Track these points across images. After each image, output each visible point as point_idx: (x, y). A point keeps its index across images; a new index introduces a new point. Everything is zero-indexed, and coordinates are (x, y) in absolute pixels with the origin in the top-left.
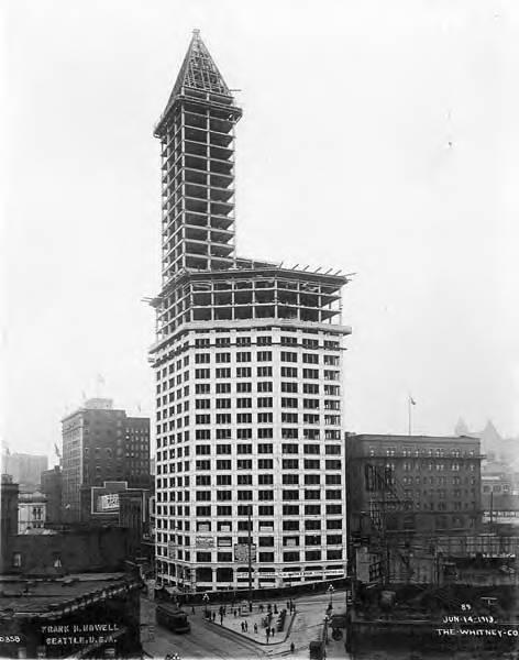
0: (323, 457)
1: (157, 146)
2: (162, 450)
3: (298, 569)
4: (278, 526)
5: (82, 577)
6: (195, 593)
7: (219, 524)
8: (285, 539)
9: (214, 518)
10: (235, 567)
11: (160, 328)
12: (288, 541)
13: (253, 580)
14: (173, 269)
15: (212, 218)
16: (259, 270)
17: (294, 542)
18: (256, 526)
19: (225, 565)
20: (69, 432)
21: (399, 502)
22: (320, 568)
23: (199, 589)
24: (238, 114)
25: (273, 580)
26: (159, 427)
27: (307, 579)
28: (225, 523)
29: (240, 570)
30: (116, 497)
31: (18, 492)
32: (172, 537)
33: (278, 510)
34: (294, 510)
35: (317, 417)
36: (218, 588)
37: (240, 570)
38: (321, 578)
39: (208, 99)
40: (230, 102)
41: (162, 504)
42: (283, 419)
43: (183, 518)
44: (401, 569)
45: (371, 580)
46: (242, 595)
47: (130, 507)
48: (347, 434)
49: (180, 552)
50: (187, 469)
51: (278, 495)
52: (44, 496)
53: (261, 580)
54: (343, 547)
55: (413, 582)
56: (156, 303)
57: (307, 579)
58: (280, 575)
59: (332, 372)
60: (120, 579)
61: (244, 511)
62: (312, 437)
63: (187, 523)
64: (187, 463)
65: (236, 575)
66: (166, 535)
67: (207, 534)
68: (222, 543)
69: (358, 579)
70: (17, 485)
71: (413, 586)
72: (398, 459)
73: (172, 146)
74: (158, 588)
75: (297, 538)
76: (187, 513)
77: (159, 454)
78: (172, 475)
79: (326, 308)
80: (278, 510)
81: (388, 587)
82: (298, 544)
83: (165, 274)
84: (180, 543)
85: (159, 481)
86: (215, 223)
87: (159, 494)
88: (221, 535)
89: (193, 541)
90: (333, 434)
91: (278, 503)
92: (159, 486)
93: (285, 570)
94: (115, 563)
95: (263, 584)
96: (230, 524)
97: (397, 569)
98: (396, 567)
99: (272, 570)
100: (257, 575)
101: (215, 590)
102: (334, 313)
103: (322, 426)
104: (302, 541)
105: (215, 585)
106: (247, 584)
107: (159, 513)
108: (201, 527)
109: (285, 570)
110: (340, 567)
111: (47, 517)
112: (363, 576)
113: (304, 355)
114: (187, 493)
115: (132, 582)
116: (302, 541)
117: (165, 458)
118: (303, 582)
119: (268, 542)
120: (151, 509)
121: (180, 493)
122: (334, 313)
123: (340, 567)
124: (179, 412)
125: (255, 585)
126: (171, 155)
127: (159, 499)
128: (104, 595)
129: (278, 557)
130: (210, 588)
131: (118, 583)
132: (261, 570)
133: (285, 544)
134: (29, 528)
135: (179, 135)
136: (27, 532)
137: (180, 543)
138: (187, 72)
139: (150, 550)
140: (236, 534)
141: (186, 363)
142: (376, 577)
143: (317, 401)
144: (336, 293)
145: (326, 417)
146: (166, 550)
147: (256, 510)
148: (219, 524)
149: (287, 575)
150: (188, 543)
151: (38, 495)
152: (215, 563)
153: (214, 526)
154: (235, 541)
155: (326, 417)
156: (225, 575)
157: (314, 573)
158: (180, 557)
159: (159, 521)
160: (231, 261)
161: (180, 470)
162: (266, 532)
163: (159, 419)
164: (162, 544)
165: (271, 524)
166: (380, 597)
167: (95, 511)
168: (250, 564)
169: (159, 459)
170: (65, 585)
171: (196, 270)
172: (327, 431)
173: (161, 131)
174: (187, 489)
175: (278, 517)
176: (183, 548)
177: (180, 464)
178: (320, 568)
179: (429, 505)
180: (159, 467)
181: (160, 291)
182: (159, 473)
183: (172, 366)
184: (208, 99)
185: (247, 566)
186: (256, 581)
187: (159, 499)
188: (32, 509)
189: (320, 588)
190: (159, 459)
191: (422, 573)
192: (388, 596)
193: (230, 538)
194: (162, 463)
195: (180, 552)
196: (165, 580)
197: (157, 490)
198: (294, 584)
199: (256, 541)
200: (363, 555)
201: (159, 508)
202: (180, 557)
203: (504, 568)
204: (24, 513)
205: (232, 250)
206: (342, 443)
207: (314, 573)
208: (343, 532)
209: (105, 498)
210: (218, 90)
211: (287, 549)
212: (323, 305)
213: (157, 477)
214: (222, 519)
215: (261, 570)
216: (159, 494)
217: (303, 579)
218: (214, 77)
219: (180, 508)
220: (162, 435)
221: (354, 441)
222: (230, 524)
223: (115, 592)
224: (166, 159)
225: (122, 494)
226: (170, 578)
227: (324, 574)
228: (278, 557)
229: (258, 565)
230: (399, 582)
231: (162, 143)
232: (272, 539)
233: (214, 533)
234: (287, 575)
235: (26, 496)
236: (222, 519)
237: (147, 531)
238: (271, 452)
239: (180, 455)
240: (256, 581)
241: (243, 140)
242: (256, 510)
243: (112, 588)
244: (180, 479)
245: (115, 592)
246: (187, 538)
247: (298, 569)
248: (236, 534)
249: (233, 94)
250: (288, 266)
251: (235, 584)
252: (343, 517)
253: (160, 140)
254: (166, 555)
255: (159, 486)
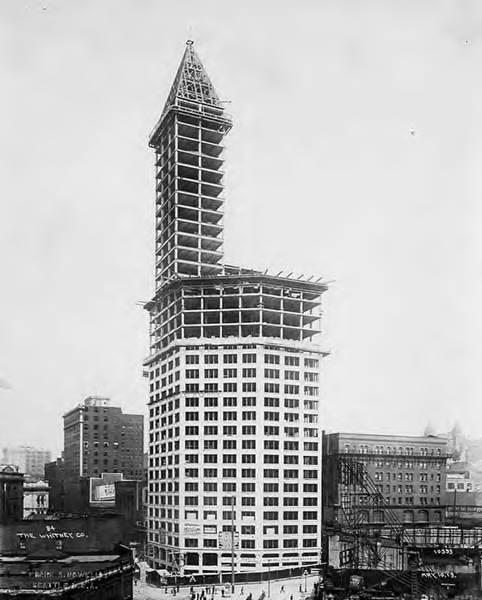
0: (301, 453)
1: (151, 155)
2: (154, 444)
3: (277, 555)
4: (259, 515)
5: (81, 559)
6: (182, 575)
7: (206, 513)
8: (265, 528)
9: (201, 508)
10: (220, 553)
11: (153, 331)
12: (268, 530)
13: (235, 565)
14: (165, 274)
15: (203, 226)
16: (247, 276)
17: (273, 530)
18: (239, 515)
19: (210, 550)
20: (71, 422)
21: (369, 495)
22: (296, 555)
23: (186, 572)
24: (228, 126)
25: (254, 565)
26: (152, 423)
27: (284, 564)
28: (210, 513)
29: (224, 555)
30: (113, 487)
31: (23, 481)
32: (163, 524)
33: (259, 501)
34: (274, 502)
35: (297, 416)
36: (204, 571)
37: (224, 555)
38: (297, 564)
39: (200, 110)
40: (221, 114)
41: (154, 494)
42: (266, 418)
43: (173, 508)
44: (369, 555)
45: (342, 564)
46: (227, 578)
47: (127, 495)
48: (323, 432)
49: (170, 538)
50: (177, 462)
51: (259, 488)
52: (47, 485)
53: (242, 565)
54: (318, 536)
55: (379, 568)
56: (149, 307)
57: (284, 564)
58: (260, 560)
59: (311, 374)
60: (114, 561)
61: (227, 501)
62: (291, 435)
63: (177, 512)
64: (177, 457)
65: (221, 560)
66: (157, 523)
67: (194, 521)
68: (208, 530)
69: (330, 564)
70: (22, 475)
71: (379, 571)
72: (371, 457)
73: (165, 156)
74: (151, 570)
75: (276, 528)
76: (177, 503)
77: (151, 448)
78: (163, 468)
79: (307, 313)
80: (259, 501)
81: (357, 572)
82: (276, 532)
83: (159, 279)
84: (170, 529)
85: (151, 473)
86: (206, 231)
87: (151, 485)
88: (206, 523)
89: (181, 528)
90: (311, 432)
91: (259, 495)
92: (151, 477)
93: (265, 556)
94: (112, 548)
95: (245, 568)
96: (215, 513)
97: (366, 556)
98: (364, 555)
99: (253, 556)
100: (239, 560)
101: (201, 573)
102: (317, 318)
103: (301, 424)
104: (281, 530)
105: (201, 568)
106: (230, 569)
107: (151, 501)
108: (188, 514)
109: (265, 556)
110: (316, 554)
111: (50, 506)
112: (335, 562)
113: (286, 358)
114: (177, 484)
115: (126, 564)
116: (281, 530)
117: (157, 452)
118: (281, 568)
119: (247, 530)
120: (144, 499)
121: (170, 484)
122: (317, 318)
123: (316, 554)
124: (171, 409)
125: (239, 570)
126: (164, 164)
127: (151, 490)
128: (101, 575)
129: (259, 545)
130: (197, 571)
131: (114, 564)
132: (243, 556)
133: (265, 533)
134: (33, 513)
135: (173, 145)
136: (31, 518)
137: (170, 529)
138: (181, 82)
139: (141, 536)
140: (220, 522)
141: (178, 364)
142: (346, 563)
143: (297, 401)
144: (314, 301)
145: (306, 416)
146: (157, 535)
147: (239, 501)
148: (206, 513)
149: (266, 561)
150: (177, 530)
151: (41, 484)
152: (201, 550)
153: (201, 515)
154: (220, 529)
155: (306, 416)
156: (211, 559)
157: (291, 560)
158: (170, 543)
159: (151, 510)
160: (218, 267)
161: (170, 463)
162: (248, 521)
163: (152, 416)
164: (155, 531)
165: (253, 514)
166: (349, 580)
167: (93, 495)
168: (232, 550)
169: (152, 453)
170: (66, 565)
171: (185, 276)
172: (305, 429)
173: (155, 141)
174: (177, 481)
175: (260, 508)
176: (173, 534)
177: (170, 457)
178: (296, 555)
179: (397, 501)
180: (151, 460)
181: (154, 296)
182: (151, 465)
183: (164, 367)
184: (200, 110)
185: (230, 552)
186: (239, 565)
187: (151, 490)
188: (36, 497)
189: (297, 573)
190: (152, 453)
191: (388, 560)
192: (356, 580)
193: (215, 526)
194: (154, 456)
195: (170, 538)
196: (157, 564)
197: (150, 482)
198: (273, 569)
199: (239, 529)
200: (335, 544)
201: (151, 497)
202: (170, 543)
203: (463, 558)
204: (29, 501)
205: (221, 257)
206: (319, 440)
207: (291, 560)
208: (318, 522)
209: (101, 489)
210: (209, 101)
211: (267, 538)
212: (304, 311)
213: (150, 469)
214: (209, 508)
215: (243, 556)
216: (151, 485)
217: (281, 565)
218: (206, 89)
219: (170, 498)
220: (155, 430)
221: (331, 441)
222: (215, 513)
223: (110, 573)
224: (160, 168)
225: (117, 484)
226: (160, 562)
227: (300, 560)
228: (259, 545)
229: (240, 551)
230: (365, 568)
231: (158, 152)
232: (253, 528)
233: (201, 522)
234: (266, 561)
235: (30, 485)
236: (209, 508)
237: (142, 520)
238: (254, 447)
239: (170, 450)
240: (239, 565)
241: (237, 157)
242: (239, 501)
243: (108, 569)
244: (170, 471)
245: (110, 573)
246: (177, 526)
247: (277, 555)
248: (220, 522)
249: (224, 105)
250: (273, 273)
251: (219, 568)
252: (318, 509)
253: (155, 150)
254: (157, 540)
255: (151, 477)
